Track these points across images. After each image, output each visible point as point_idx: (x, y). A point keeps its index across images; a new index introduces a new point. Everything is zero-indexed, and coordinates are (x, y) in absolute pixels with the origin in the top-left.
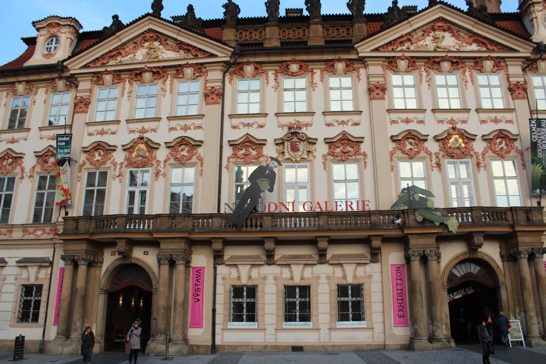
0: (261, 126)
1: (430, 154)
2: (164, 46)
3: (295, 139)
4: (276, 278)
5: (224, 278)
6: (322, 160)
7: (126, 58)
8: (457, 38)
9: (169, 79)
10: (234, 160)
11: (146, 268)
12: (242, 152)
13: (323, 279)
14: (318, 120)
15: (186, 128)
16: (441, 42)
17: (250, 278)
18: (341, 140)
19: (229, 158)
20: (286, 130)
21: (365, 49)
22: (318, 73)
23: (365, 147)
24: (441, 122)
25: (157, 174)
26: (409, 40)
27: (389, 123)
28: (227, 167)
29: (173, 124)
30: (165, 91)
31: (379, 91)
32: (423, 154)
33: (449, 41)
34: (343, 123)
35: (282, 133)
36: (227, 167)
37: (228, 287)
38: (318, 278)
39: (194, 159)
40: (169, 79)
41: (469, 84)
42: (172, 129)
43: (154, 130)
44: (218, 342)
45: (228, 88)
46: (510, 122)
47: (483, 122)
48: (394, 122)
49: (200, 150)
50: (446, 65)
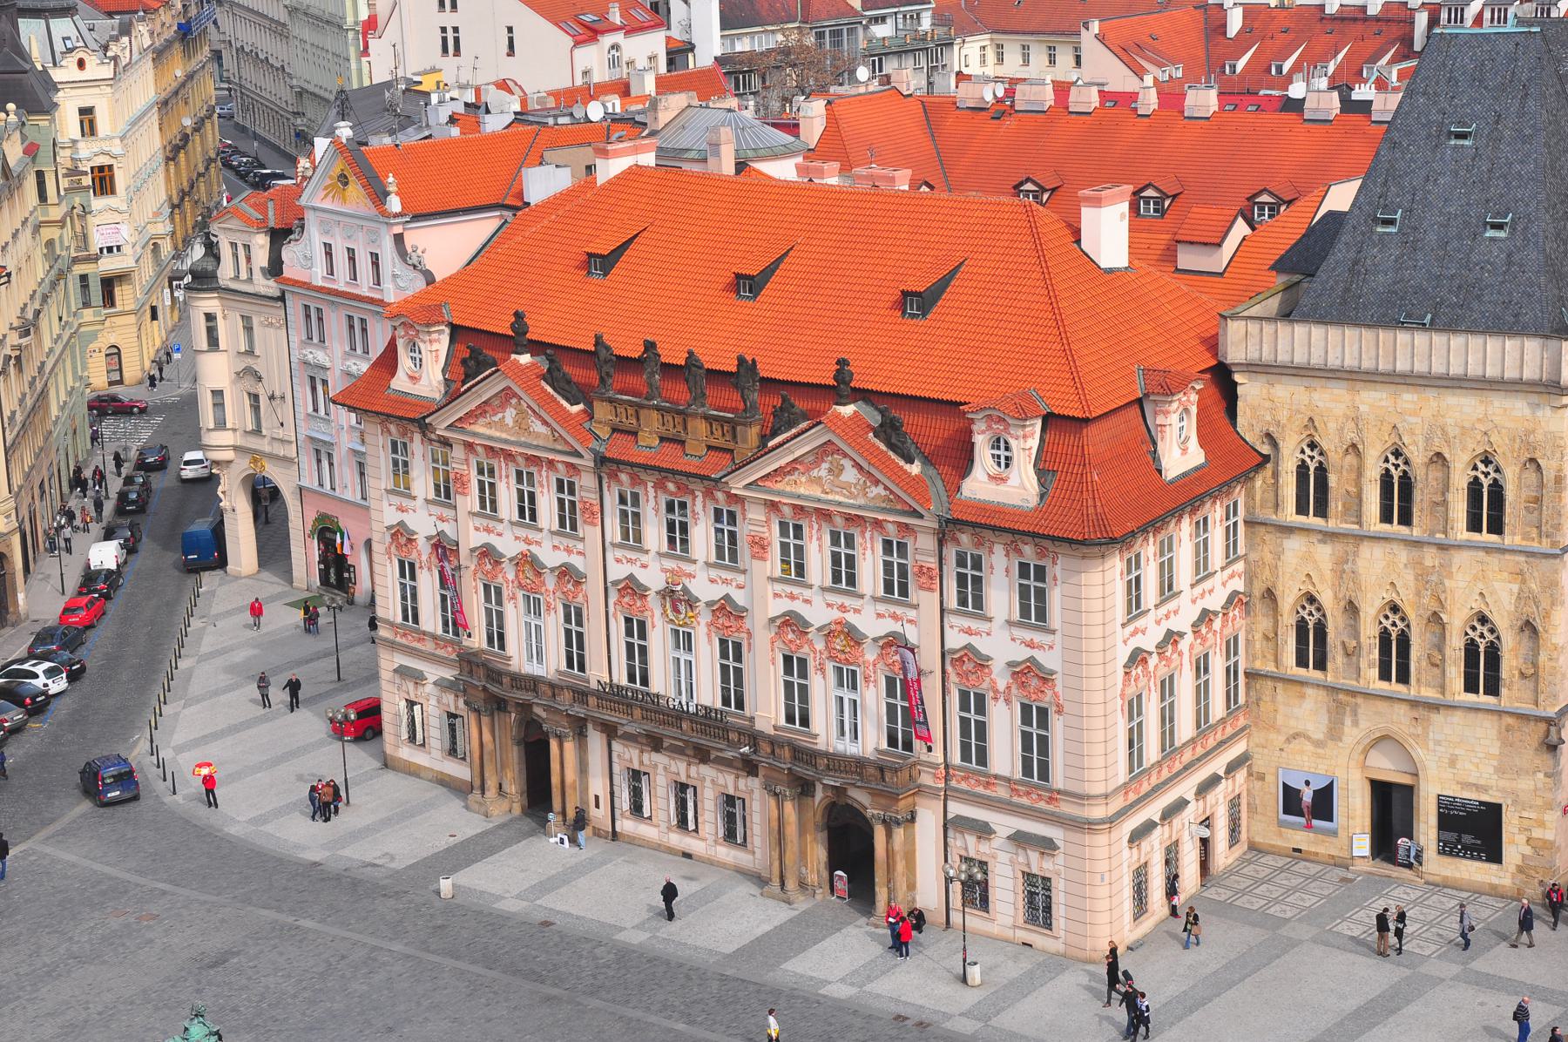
3: (677, 598)
6: (705, 630)
7: (496, 418)
12: (627, 599)
16: (838, 476)
17: (641, 763)
18: (722, 608)
21: (737, 485)
23: (747, 623)
24: (829, 605)
26: (796, 469)
27: (770, 595)
33: (850, 475)
35: (661, 585)
39: (580, 599)
41: (869, 552)
44: (618, 829)
47: (880, 616)
48: (776, 595)
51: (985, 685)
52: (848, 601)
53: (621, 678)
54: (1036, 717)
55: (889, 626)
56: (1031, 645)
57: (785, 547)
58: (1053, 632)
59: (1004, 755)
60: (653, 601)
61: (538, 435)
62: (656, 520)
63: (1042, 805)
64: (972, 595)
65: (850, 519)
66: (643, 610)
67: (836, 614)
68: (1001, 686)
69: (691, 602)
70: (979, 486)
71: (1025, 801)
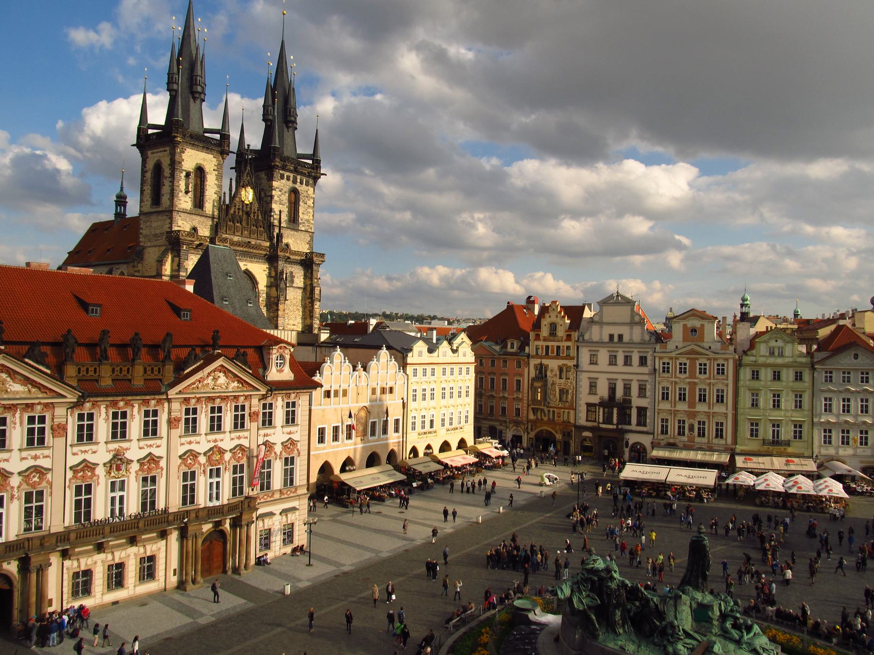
0: (94, 452)
1: (200, 464)
2: (11, 379)
4: (102, 561)
5: (67, 569)
8: (227, 378)
9: (19, 412)
10: (73, 481)
11: (9, 575)
13: (132, 556)
14: (134, 445)
15: (36, 458)
19: (70, 480)
20: (112, 454)
21: (172, 393)
22: (136, 406)
23: (163, 463)
25: (12, 497)
28: (69, 487)
29: (25, 454)
30: (15, 424)
31: (176, 423)
32: (197, 465)
33: (222, 379)
34: (151, 446)
35: (108, 457)
36: (69, 487)
37: (71, 574)
38: (129, 556)
39: (44, 484)
40: (19, 412)
42: (23, 459)
43: (7, 460)
45: (69, 418)
46: (246, 438)
49: (49, 476)
50: (218, 400)
51: (273, 454)
52: (218, 436)
53: (69, 520)
54: (289, 461)
55: (236, 442)
56: (290, 433)
57: (187, 420)
58: (297, 425)
59: (277, 481)
60: (100, 471)
61: (17, 392)
62: (106, 425)
63: (292, 495)
64: (268, 421)
65: (224, 399)
66: (94, 475)
67: (212, 445)
68: (278, 453)
69: (130, 462)
70: (274, 374)
71: (286, 496)
